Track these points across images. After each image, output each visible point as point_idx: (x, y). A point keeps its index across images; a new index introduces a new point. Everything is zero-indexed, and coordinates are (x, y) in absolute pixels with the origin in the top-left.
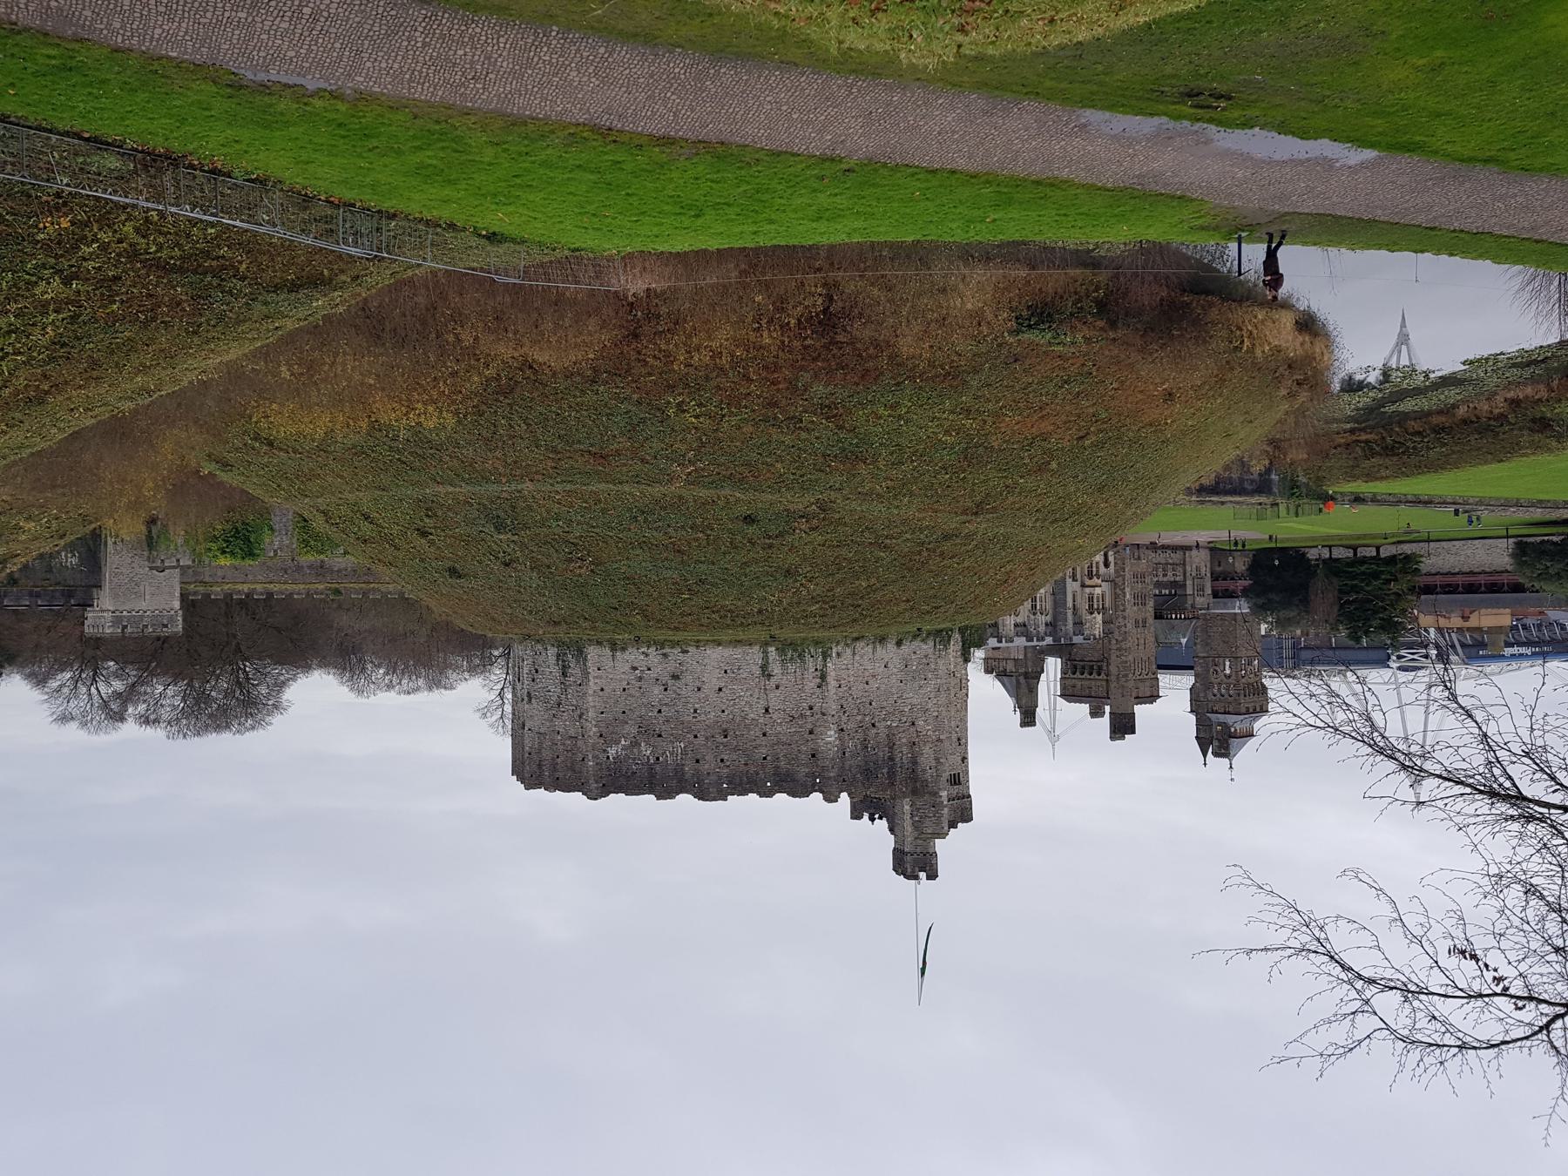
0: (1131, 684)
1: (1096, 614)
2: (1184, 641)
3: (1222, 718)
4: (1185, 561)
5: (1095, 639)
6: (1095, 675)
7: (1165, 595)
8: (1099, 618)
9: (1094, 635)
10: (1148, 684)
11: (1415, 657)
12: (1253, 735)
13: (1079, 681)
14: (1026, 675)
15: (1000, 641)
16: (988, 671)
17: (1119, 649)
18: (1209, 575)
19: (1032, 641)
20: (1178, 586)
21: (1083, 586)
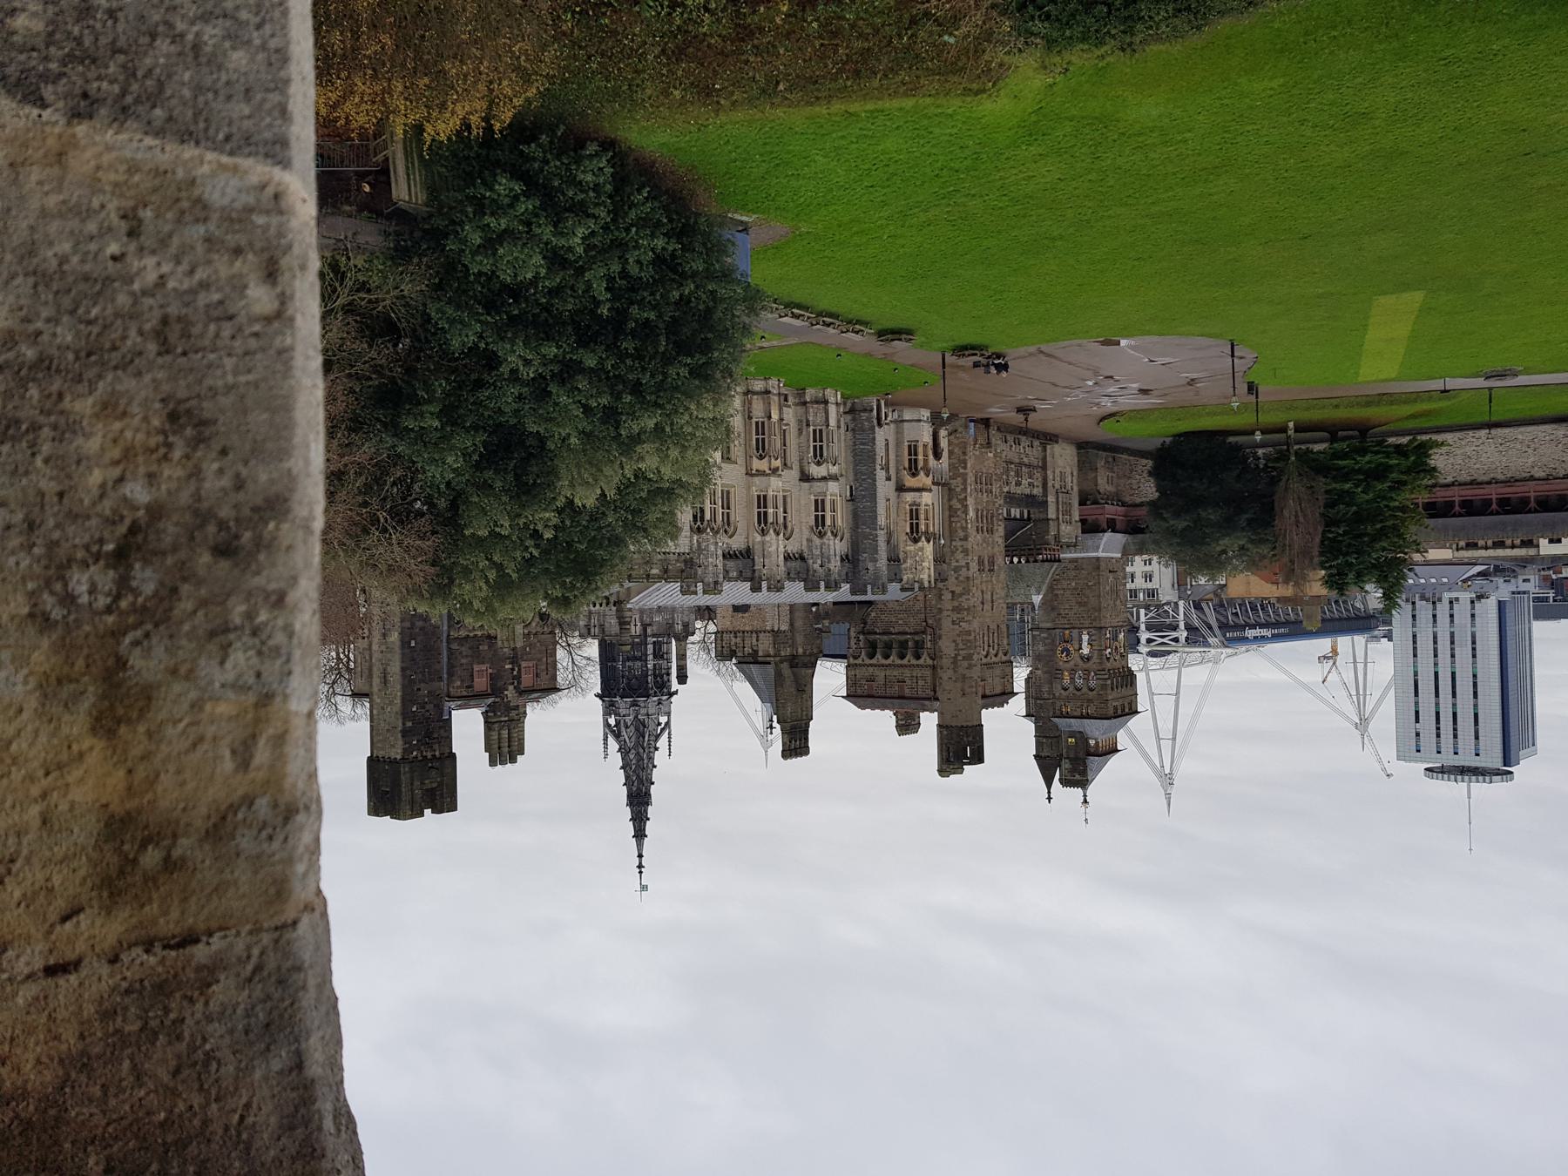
0: (976, 673)
1: (923, 543)
2: (1037, 599)
3: (1075, 724)
4: (1044, 459)
5: (922, 588)
6: (909, 658)
7: (1015, 519)
8: (929, 548)
9: (921, 582)
10: (998, 672)
11: (1165, 640)
12: (1114, 750)
13: (882, 670)
14: (793, 661)
15: (756, 589)
16: (724, 654)
17: (957, 609)
18: (1076, 488)
19: (817, 588)
20: (1035, 503)
21: (901, 488)
